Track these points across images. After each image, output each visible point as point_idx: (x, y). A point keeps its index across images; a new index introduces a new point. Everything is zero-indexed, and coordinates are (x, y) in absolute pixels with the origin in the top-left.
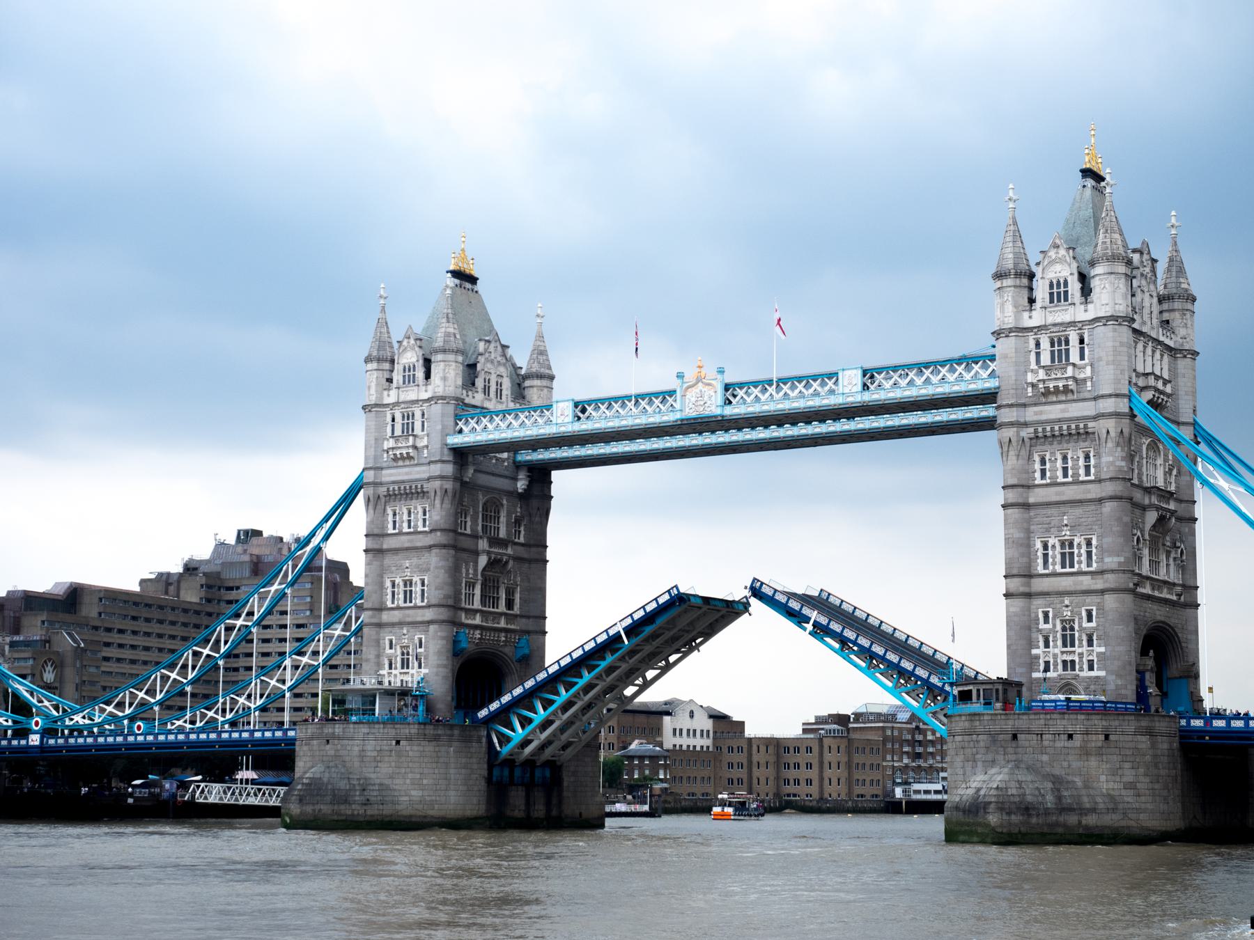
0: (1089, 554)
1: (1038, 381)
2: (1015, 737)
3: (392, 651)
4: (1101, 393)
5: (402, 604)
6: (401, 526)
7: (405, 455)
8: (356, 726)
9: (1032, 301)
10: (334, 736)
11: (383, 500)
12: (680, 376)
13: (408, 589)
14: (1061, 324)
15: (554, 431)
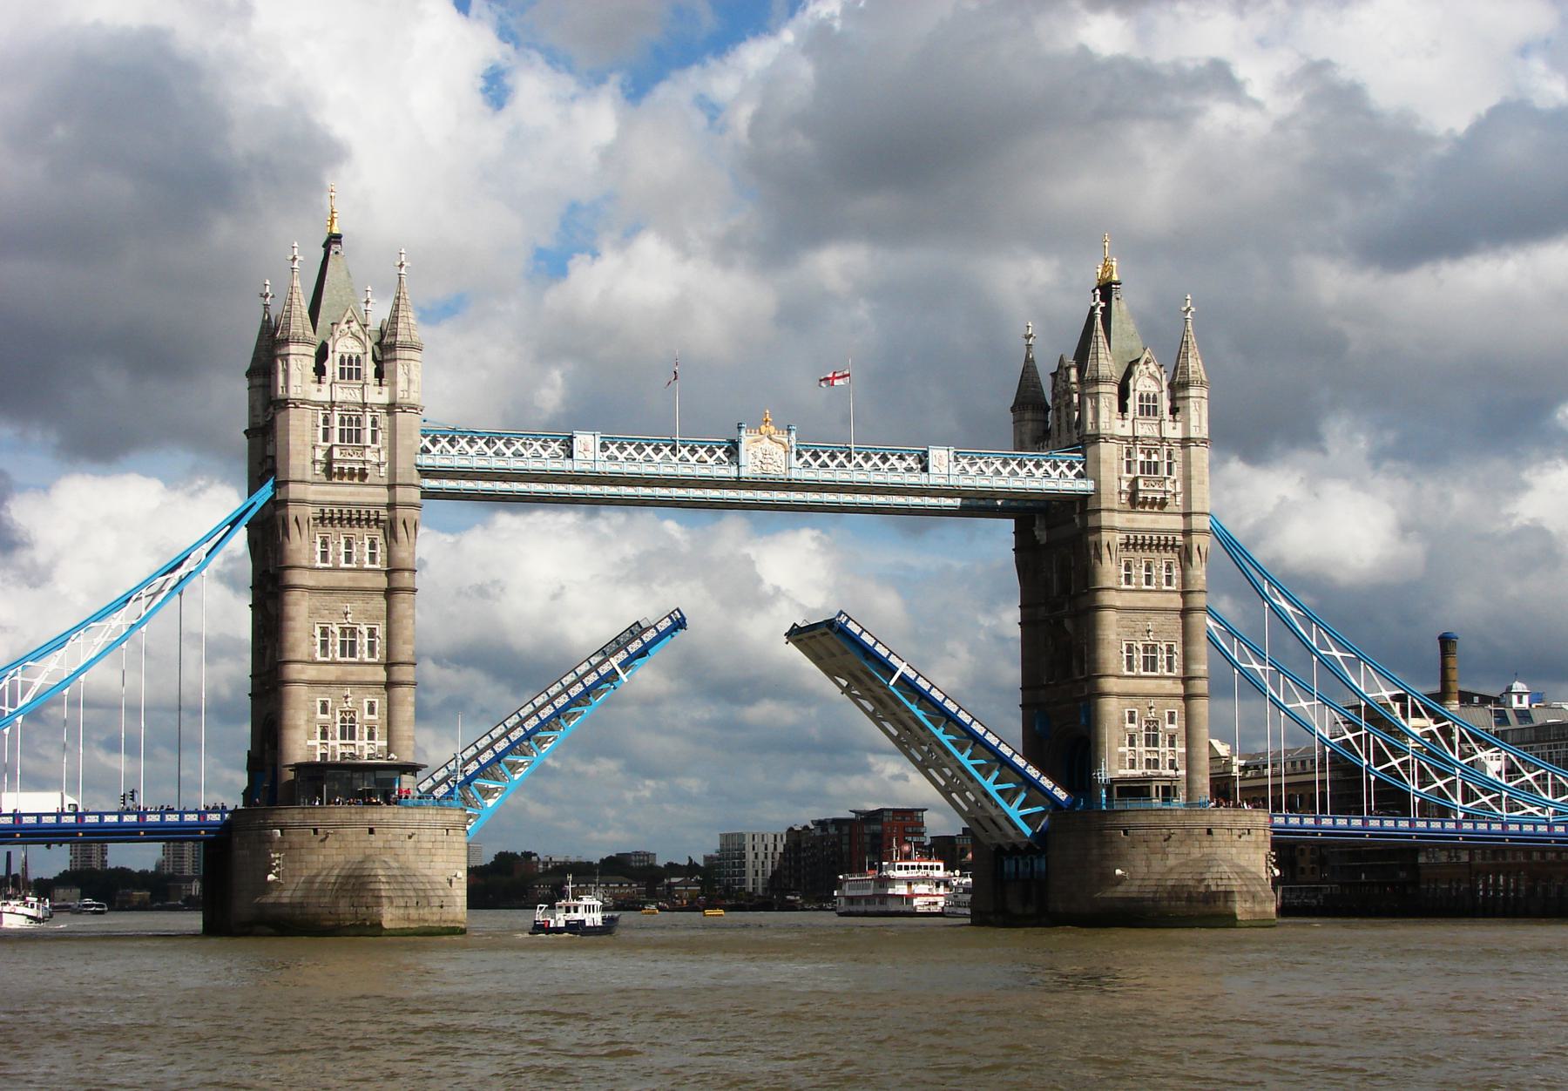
0: (1170, 660)
1: (1141, 490)
2: (1209, 832)
3: (328, 717)
4: (1193, 510)
5: (339, 658)
6: (336, 559)
7: (357, 471)
8: (410, 811)
9: (1123, 408)
10: (381, 824)
11: (311, 521)
12: (740, 428)
13: (348, 639)
14: (1154, 438)
15: (576, 469)
